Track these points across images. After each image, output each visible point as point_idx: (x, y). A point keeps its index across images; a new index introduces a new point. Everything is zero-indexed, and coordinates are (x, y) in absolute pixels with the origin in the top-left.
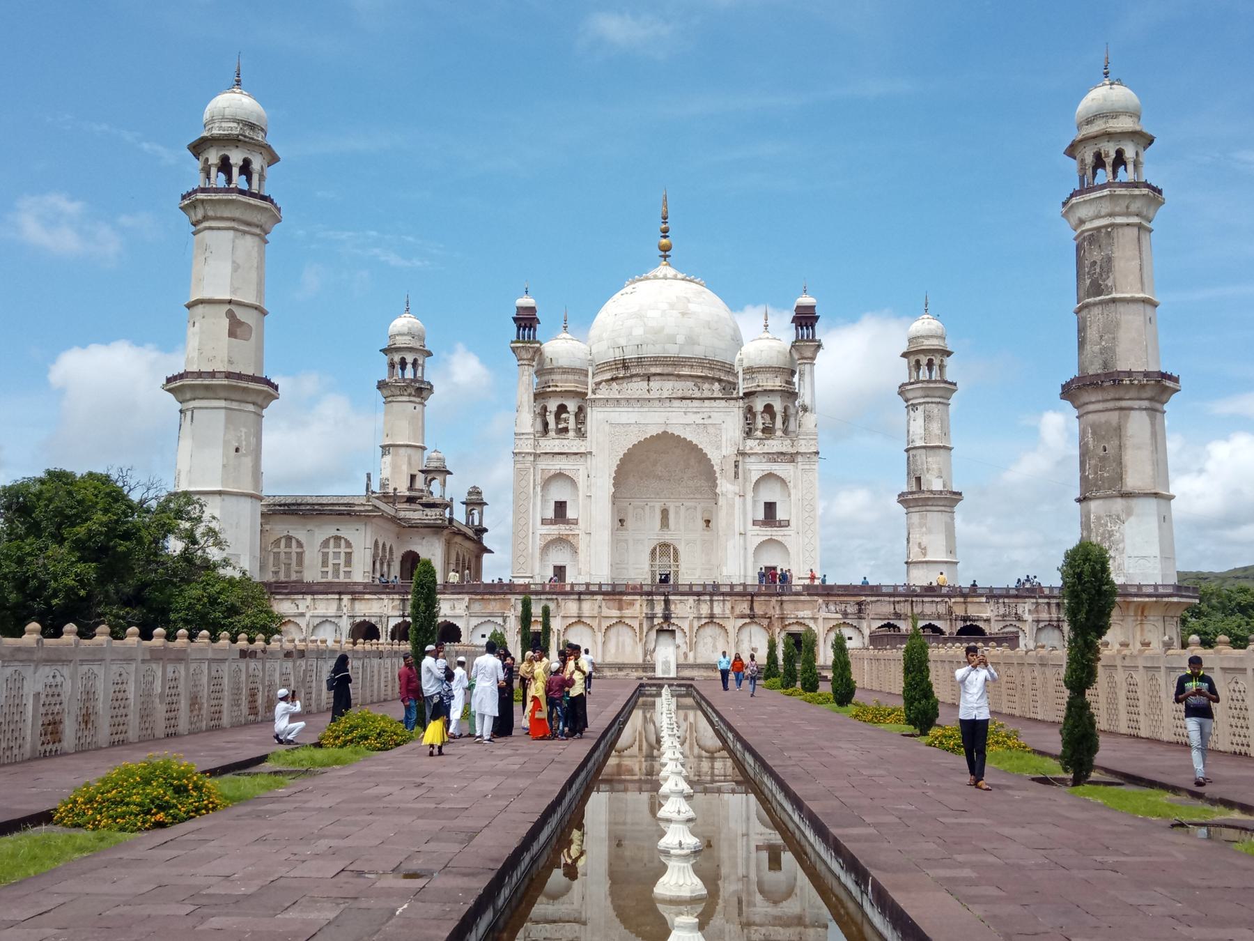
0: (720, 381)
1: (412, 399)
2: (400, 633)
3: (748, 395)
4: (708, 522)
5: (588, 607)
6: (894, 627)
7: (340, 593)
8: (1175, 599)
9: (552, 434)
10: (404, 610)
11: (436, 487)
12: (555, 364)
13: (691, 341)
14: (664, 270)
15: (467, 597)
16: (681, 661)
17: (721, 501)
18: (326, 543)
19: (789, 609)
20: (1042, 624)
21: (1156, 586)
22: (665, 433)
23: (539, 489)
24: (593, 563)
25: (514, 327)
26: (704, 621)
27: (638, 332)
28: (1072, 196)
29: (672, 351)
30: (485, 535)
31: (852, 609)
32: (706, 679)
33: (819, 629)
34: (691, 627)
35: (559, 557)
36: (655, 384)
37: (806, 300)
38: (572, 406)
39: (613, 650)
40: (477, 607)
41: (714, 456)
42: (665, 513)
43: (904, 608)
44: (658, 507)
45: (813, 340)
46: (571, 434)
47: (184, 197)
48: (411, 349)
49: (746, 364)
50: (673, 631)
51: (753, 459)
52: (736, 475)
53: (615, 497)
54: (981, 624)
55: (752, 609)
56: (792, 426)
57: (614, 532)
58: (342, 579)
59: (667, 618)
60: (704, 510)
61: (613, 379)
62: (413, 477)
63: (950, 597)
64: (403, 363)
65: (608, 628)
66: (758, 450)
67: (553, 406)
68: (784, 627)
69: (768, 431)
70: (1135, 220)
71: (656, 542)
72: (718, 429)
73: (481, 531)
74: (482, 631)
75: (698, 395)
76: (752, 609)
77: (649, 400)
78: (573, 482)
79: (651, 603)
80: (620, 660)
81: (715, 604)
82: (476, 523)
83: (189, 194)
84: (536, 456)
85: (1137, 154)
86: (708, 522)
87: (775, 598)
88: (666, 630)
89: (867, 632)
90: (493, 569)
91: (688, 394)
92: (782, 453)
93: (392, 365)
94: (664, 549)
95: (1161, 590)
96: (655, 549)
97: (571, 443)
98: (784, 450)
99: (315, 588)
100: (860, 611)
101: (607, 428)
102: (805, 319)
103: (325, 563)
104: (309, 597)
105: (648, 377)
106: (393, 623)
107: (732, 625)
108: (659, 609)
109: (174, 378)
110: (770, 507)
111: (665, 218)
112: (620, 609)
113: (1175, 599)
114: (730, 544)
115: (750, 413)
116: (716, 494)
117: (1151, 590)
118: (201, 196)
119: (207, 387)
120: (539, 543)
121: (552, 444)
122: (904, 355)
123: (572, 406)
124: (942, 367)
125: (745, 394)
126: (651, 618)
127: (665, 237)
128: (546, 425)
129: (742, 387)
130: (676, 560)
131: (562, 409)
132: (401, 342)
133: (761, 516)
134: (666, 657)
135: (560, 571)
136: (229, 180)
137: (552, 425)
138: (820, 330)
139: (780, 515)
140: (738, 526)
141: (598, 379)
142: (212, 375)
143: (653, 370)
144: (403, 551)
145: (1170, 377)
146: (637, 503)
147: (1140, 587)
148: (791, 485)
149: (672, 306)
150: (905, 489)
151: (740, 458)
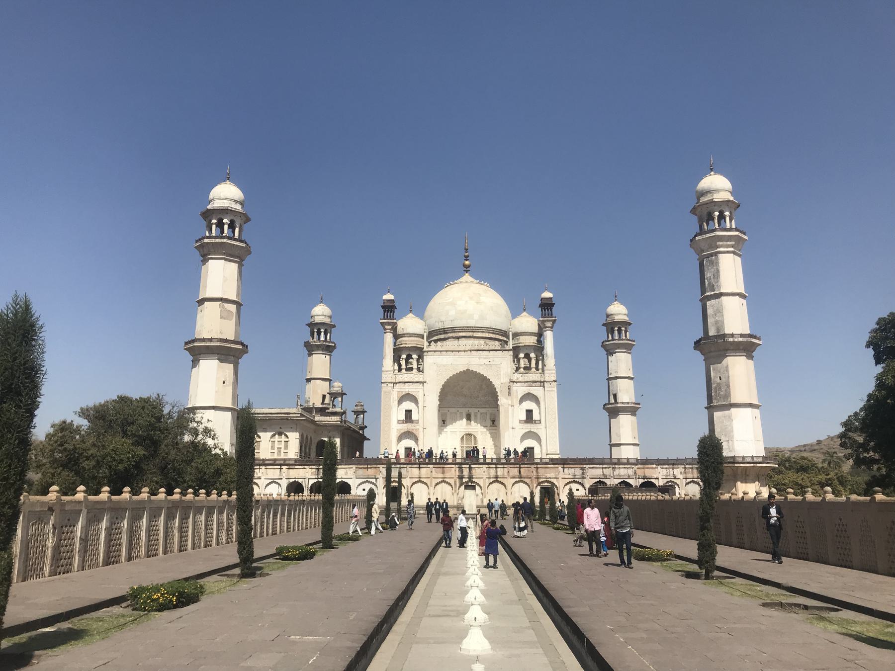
2: (315, 489)
4: (493, 421)
5: (425, 471)
6: (603, 483)
7: (281, 465)
8: (764, 465)
9: (404, 371)
10: (318, 475)
12: (405, 332)
15: (354, 467)
16: (479, 504)
19: (541, 472)
20: (688, 480)
21: (753, 457)
23: (396, 403)
25: (382, 311)
26: (492, 480)
27: (452, 313)
28: (696, 236)
29: (472, 323)
31: (578, 472)
33: (560, 483)
34: (484, 483)
35: (408, 443)
36: (463, 342)
37: (547, 295)
38: (415, 356)
40: (361, 472)
41: (497, 383)
43: (608, 472)
46: (415, 371)
48: (323, 324)
52: (509, 393)
53: (440, 407)
55: (520, 472)
56: (540, 366)
58: (282, 456)
59: (470, 477)
60: (491, 414)
62: (324, 397)
64: (319, 333)
66: (521, 379)
68: (539, 484)
69: (528, 368)
70: (732, 249)
73: (363, 428)
74: (363, 486)
76: (520, 472)
78: (414, 400)
79: (461, 469)
82: (360, 422)
83: (200, 240)
84: (394, 383)
86: (493, 421)
87: (533, 466)
88: (470, 486)
89: (587, 486)
90: (369, 451)
91: (482, 347)
95: (755, 459)
98: (536, 379)
99: (267, 462)
100: (583, 473)
102: (547, 306)
103: (273, 448)
104: (263, 467)
105: (458, 338)
106: (312, 482)
107: (509, 482)
109: (190, 342)
110: (529, 412)
112: (443, 473)
113: (764, 465)
114: (506, 434)
117: (750, 460)
122: (604, 325)
126: (461, 478)
128: (400, 366)
130: (475, 443)
132: (318, 319)
133: (523, 417)
135: (408, 450)
136: (222, 232)
137: (404, 366)
139: (536, 416)
142: (211, 340)
144: (318, 440)
147: (743, 458)
151: (511, 384)
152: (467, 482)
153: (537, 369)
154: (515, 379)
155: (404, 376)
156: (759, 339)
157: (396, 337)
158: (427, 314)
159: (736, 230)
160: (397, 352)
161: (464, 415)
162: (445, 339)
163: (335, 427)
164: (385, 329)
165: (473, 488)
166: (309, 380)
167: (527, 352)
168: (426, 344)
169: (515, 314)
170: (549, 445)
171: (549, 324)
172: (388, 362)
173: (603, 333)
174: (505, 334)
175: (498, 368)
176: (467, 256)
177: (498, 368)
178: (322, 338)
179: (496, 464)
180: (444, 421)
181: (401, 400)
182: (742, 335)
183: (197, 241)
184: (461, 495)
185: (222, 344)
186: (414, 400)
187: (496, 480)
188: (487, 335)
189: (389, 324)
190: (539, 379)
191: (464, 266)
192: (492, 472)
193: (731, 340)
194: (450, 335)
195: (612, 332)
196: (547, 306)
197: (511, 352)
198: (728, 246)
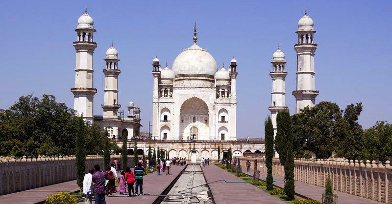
3: (218, 87)
4: (206, 121)
5: (174, 145)
13: (202, 69)
14: (195, 46)
17: (210, 115)
22: (195, 97)
23: (160, 112)
24: (174, 134)
27: (187, 67)
29: (197, 72)
36: (192, 81)
37: (234, 61)
41: (208, 104)
42: (194, 118)
43: (251, 146)
44: (192, 116)
46: (169, 97)
48: (114, 60)
49: (217, 78)
50: (196, 152)
52: (214, 109)
56: (230, 95)
57: (180, 124)
59: (194, 148)
61: (180, 80)
70: (310, 53)
72: (208, 96)
73: (139, 120)
78: (169, 111)
85: (311, 36)
86: (206, 121)
88: (194, 151)
89: (243, 152)
97: (168, 99)
100: (241, 147)
102: (234, 66)
105: (190, 79)
107: (210, 150)
108: (192, 146)
109: (74, 89)
110: (223, 117)
112: (183, 146)
115: (218, 91)
118: (79, 44)
119: (82, 92)
120: (160, 128)
121: (163, 99)
124: (283, 67)
125: (217, 86)
129: (216, 84)
132: (111, 57)
133: (220, 119)
134: (194, 158)
135: (165, 134)
140: (214, 123)
141: (176, 79)
143: (191, 78)
145: (316, 92)
146: (187, 115)
148: (229, 112)
149: (197, 59)
152: (193, 150)
153: (228, 96)
156: (318, 92)
157: (160, 79)
158: (174, 65)
159: (312, 45)
160: (160, 87)
161: (192, 118)
162: (183, 80)
163: (131, 123)
164: (154, 76)
165: (196, 152)
166: (105, 91)
167: (223, 88)
170: (231, 134)
171: (234, 76)
172: (156, 93)
173: (271, 68)
174: (212, 77)
175: (208, 96)
176: (196, 34)
178: (113, 68)
181: (162, 111)
182: (309, 91)
183: (74, 43)
184: (190, 155)
185: (88, 90)
186: (169, 111)
187: (205, 149)
188: (204, 78)
189: (156, 74)
192: (204, 146)
193: (304, 93)
194: (186, 78)
196: (234, 66)
198: (308, 52)
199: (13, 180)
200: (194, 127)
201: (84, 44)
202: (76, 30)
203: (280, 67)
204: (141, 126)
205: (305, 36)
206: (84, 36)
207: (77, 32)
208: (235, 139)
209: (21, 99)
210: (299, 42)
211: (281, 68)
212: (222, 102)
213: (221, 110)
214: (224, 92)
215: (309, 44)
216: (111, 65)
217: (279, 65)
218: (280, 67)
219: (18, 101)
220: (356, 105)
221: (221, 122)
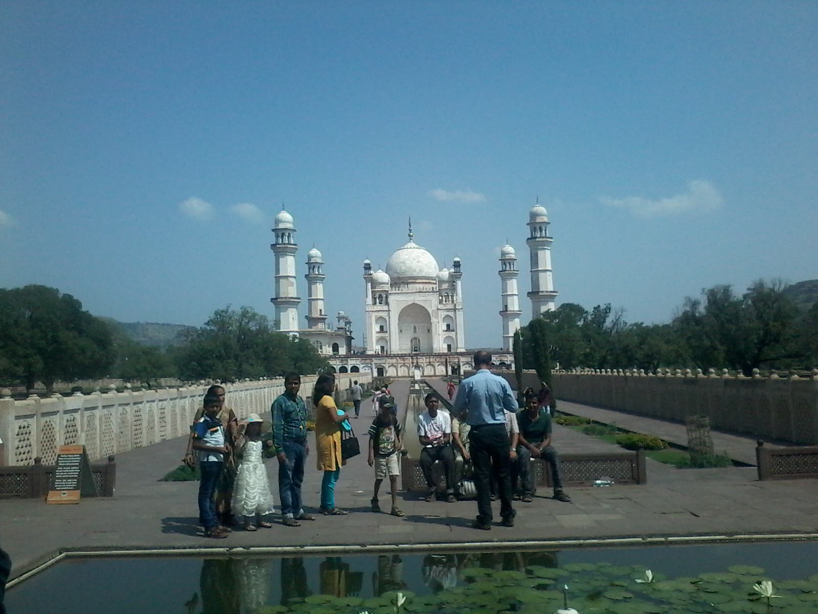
0: (431, 283)
1: (318, 281)
4: (429, 330)
5: (394, 361)
9: (378, 304)
11: (341, 321)
14: (412, 244)
15: (360, 359)
18: (314, 343)
22: (414, 303)
27: (403, 268)
29: (415, 274)
30: (352, 333)
32: (429, 380)
37: (457, 259)
38: (384, 296)
39: (402, 372)
41: (430, 310)
42: (415, 328)
45: (460, 272)
47: (272, 245)
50: (419, 367)
51: (442, 311)
54: (506, 362)
57: (399, 335)
59: (417, 363)
63: (497, 354)
65: (401, 366)
67: (377, 296)
71: (412, 337)
73: (351, 332)
75: (425, 291)
77: (408, 293)
80: (405, 375)
81: (431, 359)
86: (429, 330)
87: (447, 357)
88: (417, 367)
92: (450, 309)
93: (309, 269)
94: (415, 340)
96: (412, 340)
101: (395, 302)
102: (457, 265)
106: (340, 366)
108: (415, 361)
111: (410, 225)
114: (436, 338)
116: (431, 323)
123: (384, 296)
124: (513, 264)
126: (413, 363)
127: (411, 232)
131: (380, 295)
133: (445, 328)
134: (418, 375)
137: (378, 301)
138: (462, 269)
142: (285, 298)
150: (502, 310)
154: (439, 307)
155: (378, 307)
156: (557, 292)
161: (412, 327)
168: (390, 289)
169: (441, 270)
172: (369, 300)
175: (431, 303)
177: (431, 303)
178: (317, 273)
179: (430, 356)
180: (401, 331)
182: (547, 292)
187: (430, 364)
188: (424, 281)
190: (453, 308)
191: (409, 235)
195: (505, 264)
196: (457, 265)
197: (438, 293)
199: (237, 407)
200: (414, 338)
201: (283, 246)
202: (273, 230)
203: (510, 265)
204: (353, 338)
205: (538, 228)
206: (282, 237)
207: (274, 233)
208: (463, 350)
209: (216, 313)
210: (532, 235)
211: (512, 265)
212: (445, 308)
213: (445, 317)
214: (448, 296)
215: (543, 237)
216: (313, 269)
217: (509, 263)
218: (510, 265)
219: (213, 316)
220: (603, 307)
221: (446, 331)
